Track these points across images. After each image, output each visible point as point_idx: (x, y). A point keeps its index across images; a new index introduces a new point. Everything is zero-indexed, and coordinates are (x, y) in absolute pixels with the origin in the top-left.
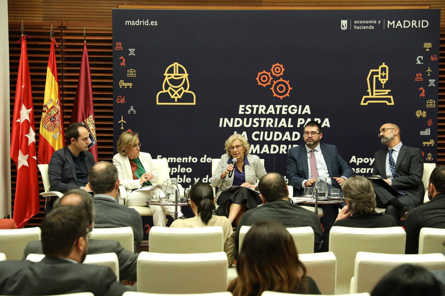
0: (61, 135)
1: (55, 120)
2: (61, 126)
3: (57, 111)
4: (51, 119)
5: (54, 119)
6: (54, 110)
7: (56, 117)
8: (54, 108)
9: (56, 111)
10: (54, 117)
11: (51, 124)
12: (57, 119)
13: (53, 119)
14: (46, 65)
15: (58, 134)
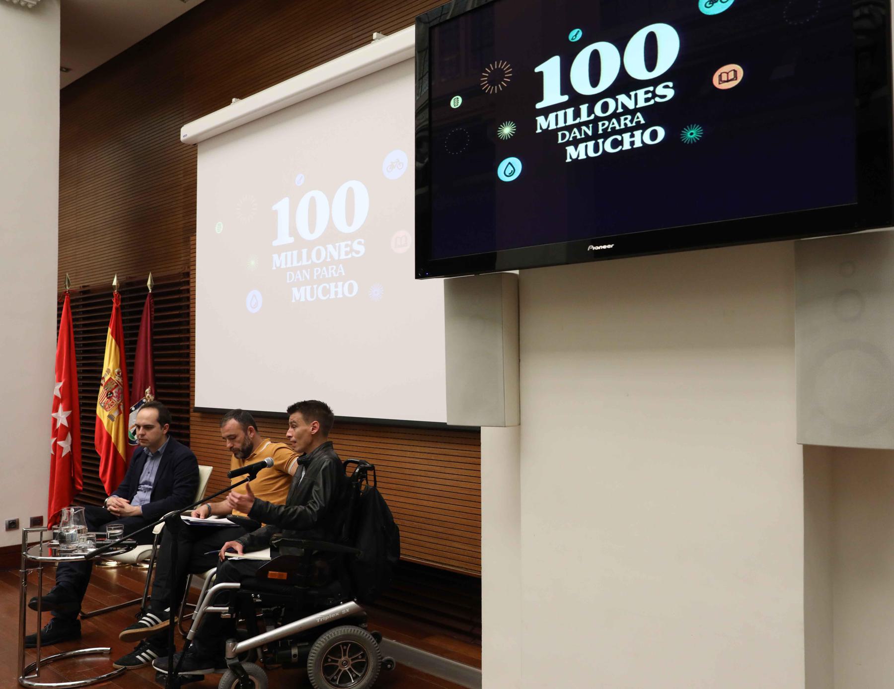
0: (122, 415)
1: (113, 396)
2: (122, 404)
3: (116, 384)
4: (107, 395)
5: (111, 395)
6: (111, 382)
7: (114, 392)
8: (111, 381)
9: (113, 384)
10: (112, 393)
11: (108, 401)
12: (115, 395)
13: (110, 394)
14: (107, 324)
15: (115, 414)
